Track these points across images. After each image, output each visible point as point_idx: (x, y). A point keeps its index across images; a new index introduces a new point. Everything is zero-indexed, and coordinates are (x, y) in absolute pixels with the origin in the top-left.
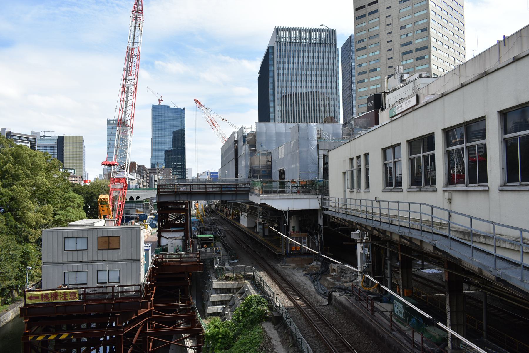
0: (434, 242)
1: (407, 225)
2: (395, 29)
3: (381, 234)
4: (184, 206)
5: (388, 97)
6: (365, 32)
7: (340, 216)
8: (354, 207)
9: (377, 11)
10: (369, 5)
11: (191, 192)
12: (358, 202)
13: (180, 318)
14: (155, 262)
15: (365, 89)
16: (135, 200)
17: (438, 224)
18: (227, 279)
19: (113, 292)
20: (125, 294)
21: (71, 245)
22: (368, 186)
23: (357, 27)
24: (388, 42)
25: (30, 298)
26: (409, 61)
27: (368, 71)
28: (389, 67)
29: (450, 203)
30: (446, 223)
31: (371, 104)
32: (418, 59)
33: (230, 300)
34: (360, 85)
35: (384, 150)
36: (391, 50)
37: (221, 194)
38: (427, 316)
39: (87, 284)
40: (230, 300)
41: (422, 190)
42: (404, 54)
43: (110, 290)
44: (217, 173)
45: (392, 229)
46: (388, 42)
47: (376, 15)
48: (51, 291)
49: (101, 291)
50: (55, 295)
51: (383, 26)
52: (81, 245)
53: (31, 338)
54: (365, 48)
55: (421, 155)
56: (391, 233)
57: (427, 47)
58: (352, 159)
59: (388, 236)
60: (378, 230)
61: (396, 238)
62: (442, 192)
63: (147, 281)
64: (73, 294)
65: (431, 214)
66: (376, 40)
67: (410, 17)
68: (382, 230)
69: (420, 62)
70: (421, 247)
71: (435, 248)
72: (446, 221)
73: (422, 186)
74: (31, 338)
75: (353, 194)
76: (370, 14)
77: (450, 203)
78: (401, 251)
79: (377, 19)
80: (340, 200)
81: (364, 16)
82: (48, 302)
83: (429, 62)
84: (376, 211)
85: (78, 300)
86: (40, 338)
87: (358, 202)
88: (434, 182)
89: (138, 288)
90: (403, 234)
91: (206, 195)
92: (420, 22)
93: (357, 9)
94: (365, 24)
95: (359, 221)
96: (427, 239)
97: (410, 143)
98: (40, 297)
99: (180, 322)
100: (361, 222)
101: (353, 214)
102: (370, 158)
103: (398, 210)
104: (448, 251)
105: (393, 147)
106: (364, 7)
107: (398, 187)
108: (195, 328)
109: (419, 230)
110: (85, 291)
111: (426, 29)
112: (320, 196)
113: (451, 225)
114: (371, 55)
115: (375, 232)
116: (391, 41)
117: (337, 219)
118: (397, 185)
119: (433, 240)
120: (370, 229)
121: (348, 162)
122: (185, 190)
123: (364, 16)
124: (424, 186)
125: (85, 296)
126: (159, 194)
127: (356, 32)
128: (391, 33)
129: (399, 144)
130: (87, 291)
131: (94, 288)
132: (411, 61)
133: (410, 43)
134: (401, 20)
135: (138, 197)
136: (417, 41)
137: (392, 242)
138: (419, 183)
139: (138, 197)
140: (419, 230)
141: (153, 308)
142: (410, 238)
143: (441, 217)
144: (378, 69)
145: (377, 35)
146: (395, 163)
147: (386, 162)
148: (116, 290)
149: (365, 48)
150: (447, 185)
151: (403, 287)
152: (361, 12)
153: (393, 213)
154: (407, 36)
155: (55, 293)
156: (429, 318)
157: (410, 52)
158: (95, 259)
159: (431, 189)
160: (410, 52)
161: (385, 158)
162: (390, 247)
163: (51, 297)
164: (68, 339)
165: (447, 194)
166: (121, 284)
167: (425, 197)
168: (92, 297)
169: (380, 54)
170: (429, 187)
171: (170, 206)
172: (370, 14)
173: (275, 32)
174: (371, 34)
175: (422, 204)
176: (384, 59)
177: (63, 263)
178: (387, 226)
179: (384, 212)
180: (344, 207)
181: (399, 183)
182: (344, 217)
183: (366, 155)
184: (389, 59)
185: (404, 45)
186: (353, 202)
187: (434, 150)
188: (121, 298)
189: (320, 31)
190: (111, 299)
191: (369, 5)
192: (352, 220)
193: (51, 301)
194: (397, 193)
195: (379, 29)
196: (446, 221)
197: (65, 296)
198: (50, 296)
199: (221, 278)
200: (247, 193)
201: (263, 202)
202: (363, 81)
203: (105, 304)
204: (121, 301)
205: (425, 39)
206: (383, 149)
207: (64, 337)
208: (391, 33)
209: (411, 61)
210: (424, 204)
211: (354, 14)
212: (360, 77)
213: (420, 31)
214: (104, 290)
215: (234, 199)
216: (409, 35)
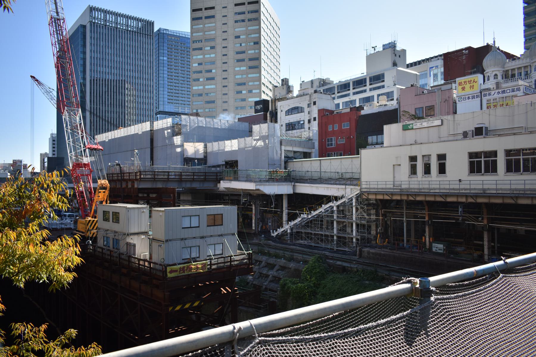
2: (231, 38)
5: (279, 104)
6: (201, 34)
9: (213, 17)
10: (206, 9)
11: (193, 179)
15: (201, 87)
21: (186, 223)
23: (194, 27)
24: (224, 47)
25: (171, 272)
26: (242, 68)
27: (203, 72)
28: (224, 71)
31: (259, 107)
32: (250, 68)
34: (197, 82)
36: (226, 55)
39: (222, 254)
42: (238, 61)
46: (224, 47)
47: (212, 20)
49: (219, 262)
51: (219, 32)
52: (195, 222)
53: (171, 309)
54: (201, 49)
57: (257, 58)
66: (212, 44)
67: (244, 29)
69: (252, 70)
74: (171, 309)
76: (206, 18)
79: (214, 24)
81: (201, 18)
82: (183, 274)
83: (260, 72)
86: (178, 308)
92: (253, 36)
93: (193, 11)
94: (201, 26)
106: (201, 9)
111: (257, 43)
112: (293, 184)
114: (206, 56)
116: (226, 47)
122: (162, 177)
123: (201, 18)
127: (192, 32)
128: (226, 39)
132: (244, 68)
133: (243, 52)
134: (236, 30)
136: (250, 52)
144: (214, 71)
145: (213, 39)
149: (201, 49)
152: (198, 13)
154: (241, 45)
157: (243, 60)
160: (243, 60)
166: (223, 256)
169: (216, 57)
172: (206, 18)
173: (89, 11)
174: (208, 37)
176: (219, 63)
184: (224, 63)
185: (238, 53)
189: (138, 20)
191: (206, 9)
193: (186, 273)
195: (215, 34)
201: (258, 187)
202: (198, 80)
205: (257, 51)
207: (196, 304)
208: (226, 39)
209: (244, 68)
211: (191, 14)
212: (195, 76)
213: (252, 44)
214: (221, 260)
215: (201, 186)
216: (243, 45)
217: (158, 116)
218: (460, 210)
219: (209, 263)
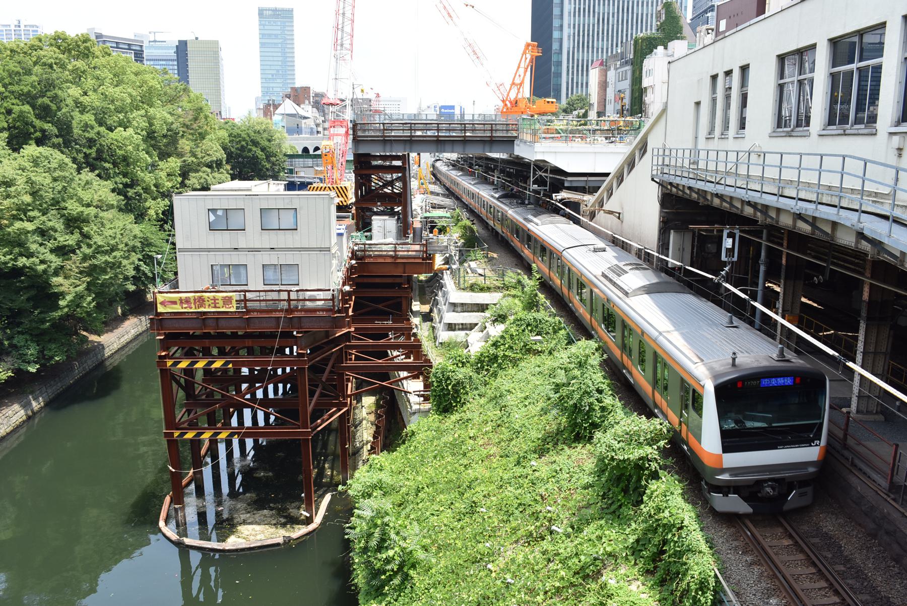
0: (861, 226)
1: (813, 197)
3: (759, 214)
4: (398, 163)
7: (684, 182)
8: (712, 167)
11: (411, 136)
12: (722, 155)
13: (396, 347)
14: (354, 255)
16: (311, 152)
17: (870, 194)
18: (472, 288)
19: (289, 300)
20: (308, 303)
22: (742, 126)
29: (900, 155)
30: (886, 190)
33: (476, 324)
35: (782, 58)
37: (465, 141)
38: (831, 352)
40: (476, 324)
41: (848, 132)
43: (284, 296)
44: (453, 107)
45: (783, 203)
48: (193, 294)
50: (201, 301)
53: (169, 363)
55: (853, 66)
56: (778, 210)
58: (714, 78)
59: (772, 218)
60: (754, 205)
61: (786, 221)
62: (886, 135)
63: (344, 284)
64: (227, 301)
65: (862, 175)
68: (763, 205)
70: (832, 236)
71: (861, 235)
72: (889, 186)
73: (848, 126)
75: (711, 141)
77: (900, 155)
78: (788, 248)
80: (687, 153)
84: (756, 171)
85: (234, 310)
87: (722, 155)
88: (873, 119)
89: (328, 295)
90: (803, 212)
91: (439, 144)
95: (720, 189)
96: (848, 219)
97: (834, 43)
98: (178, 302)
99: (395, 353)
100: (723, 193)
101: (709, 178)
102: (752, 73)
103: (799, 168)
104: (885, 240)
105: (800, 53)
107: (801, 129)
108: (419, 363)
109: (835, 206)
110: (245, 296)
113: (900, 194)
115: (748, 211)
117: (677, 186)
118: (798, 125)
119: (859, 221)
120: (740, 207)
121: (708, 81)
122: (400, 133)
124: (852, 126)
125: (245, 304)
126: (356, 141)
129: (813, 47)
130: (249, 296)
131: (259, 291)
135: (317, 149)
137: (775, 231)
138: (844, 119)
139: (317, 149)
140: (835, 206)
141: (353, 329)
142: (814, 218)
143: (880, 180)
146: (800, 82)
147: (782, 81)
148: (293, 296)
150: (898, 124)
151: (783, 311)
153: (788, 175)
155: (200, 297)
156: (833, 357)
158: (257, 245)
159: (866, 131)
161: (782, 75)
162: (768, 240)
163: (195, 303)
164: (223, 370)
165: (896, 139)
167: (855, 145)
168: (256, 305)
170: (863, 126)
171: (375, 163)
175: (847, 156)
177: (209, 250)
178: (775, 198)
179: (772, 173)
180: (692, 166)
181: (804, 120)
182: (692, 183)
183: (744, 69)
186: (712, 155)
187: (882, 56)
188: (301, 310)
190: (289, 311)
192: (706, 189)
194: (799, 139)
196: (889, 186)
197: (215, 303)
198: (192, 301)
199: (462, 286)
200: (510, 142)
203: (278, 318)
204: (303, 314)
206: (778, 56)
210: (850, 157)
214: (274, 296)
217: (709, 14)
218: (728, 243)
219: (242, 298)
